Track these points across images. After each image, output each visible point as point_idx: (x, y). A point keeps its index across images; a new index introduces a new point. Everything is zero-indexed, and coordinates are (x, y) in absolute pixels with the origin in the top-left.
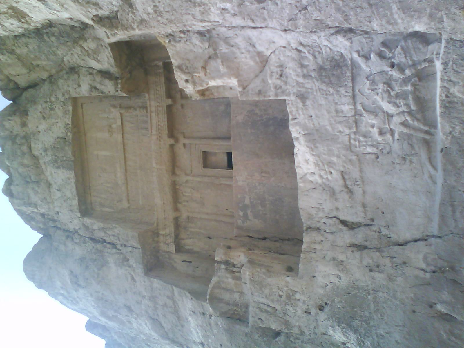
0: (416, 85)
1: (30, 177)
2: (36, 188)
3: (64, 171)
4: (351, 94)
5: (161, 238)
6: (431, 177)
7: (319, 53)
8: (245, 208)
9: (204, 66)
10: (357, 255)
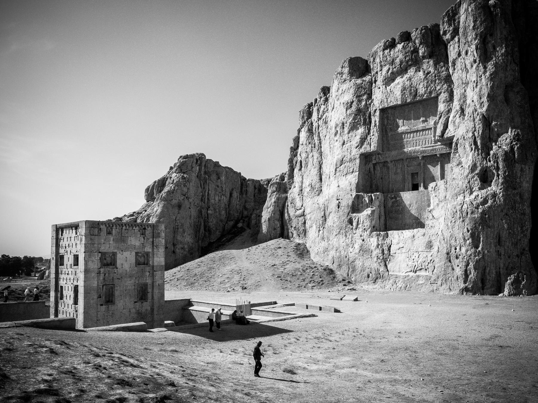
1: (395, 68)
2: (390, 72)
3: (401, 96)
5: (377, 156)
8: (395, 198)
10: (381, 252)
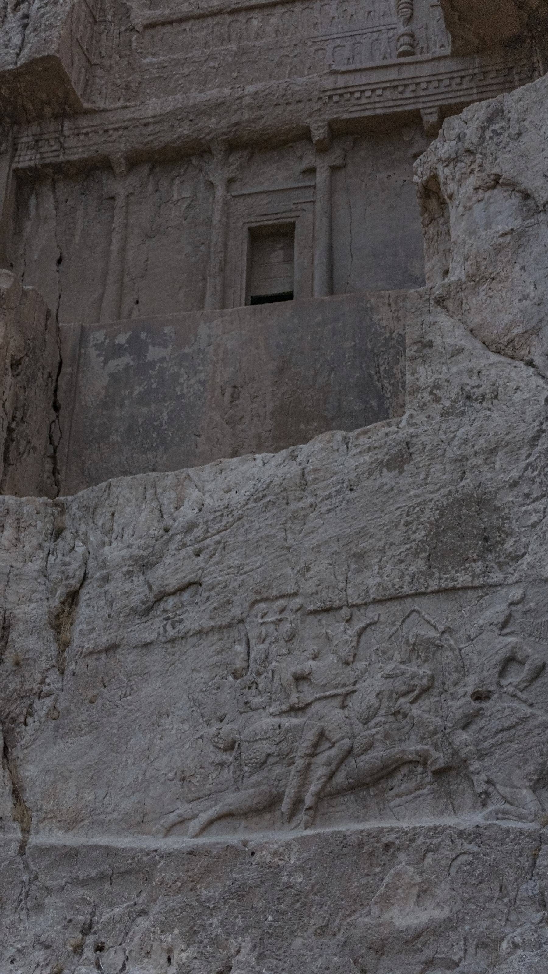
0: (425, 764)
4: (406, 589)
5: (52, 126)
6: (183, 821)
7: (527, 496)
9: (500, 181)
